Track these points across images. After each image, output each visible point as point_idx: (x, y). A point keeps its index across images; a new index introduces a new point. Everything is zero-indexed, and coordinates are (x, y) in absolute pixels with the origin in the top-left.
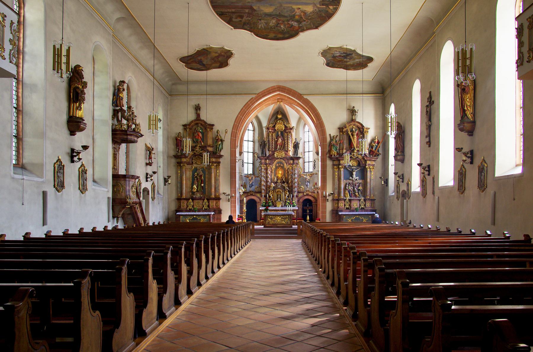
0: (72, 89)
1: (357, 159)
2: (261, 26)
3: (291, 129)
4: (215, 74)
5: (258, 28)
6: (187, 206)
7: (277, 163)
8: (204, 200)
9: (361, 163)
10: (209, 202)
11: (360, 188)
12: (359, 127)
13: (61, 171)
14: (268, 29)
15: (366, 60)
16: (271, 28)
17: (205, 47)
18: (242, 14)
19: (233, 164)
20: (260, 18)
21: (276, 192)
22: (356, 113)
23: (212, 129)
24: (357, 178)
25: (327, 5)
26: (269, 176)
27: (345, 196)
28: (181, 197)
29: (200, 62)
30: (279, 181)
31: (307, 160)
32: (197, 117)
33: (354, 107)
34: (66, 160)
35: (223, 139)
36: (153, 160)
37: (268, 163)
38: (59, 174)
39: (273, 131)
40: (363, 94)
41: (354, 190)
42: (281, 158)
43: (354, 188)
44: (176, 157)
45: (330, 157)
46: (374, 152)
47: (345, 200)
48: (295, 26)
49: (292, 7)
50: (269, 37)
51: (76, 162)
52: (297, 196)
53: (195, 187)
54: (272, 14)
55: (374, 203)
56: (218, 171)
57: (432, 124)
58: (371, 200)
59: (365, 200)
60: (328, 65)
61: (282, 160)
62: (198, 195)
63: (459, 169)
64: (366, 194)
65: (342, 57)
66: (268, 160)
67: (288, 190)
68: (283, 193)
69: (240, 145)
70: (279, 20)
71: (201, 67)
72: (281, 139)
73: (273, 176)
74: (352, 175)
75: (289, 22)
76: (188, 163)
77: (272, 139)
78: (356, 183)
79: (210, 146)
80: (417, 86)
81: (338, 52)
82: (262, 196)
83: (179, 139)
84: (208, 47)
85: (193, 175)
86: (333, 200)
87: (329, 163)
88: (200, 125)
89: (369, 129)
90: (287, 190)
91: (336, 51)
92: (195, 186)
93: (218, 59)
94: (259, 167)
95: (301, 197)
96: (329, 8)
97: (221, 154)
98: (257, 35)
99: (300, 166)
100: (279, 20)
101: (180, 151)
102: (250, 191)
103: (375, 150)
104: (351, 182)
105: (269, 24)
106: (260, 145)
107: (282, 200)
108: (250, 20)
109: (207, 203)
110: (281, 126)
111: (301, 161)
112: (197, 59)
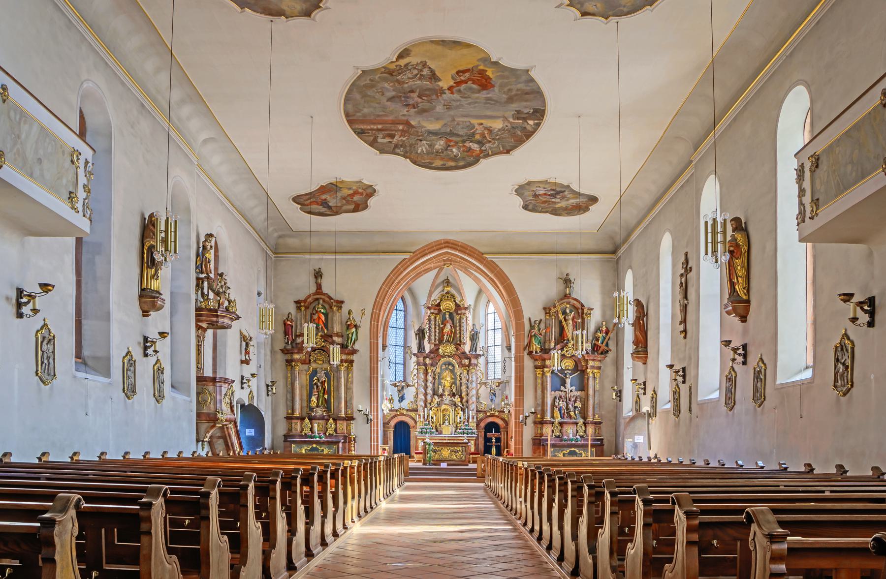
0: (146, 248)
1: (574, 358)
2: (422, 150)
3: (466, 308)
4: (346, 221)
5: (417, 153)
6: (302, 430)
8: (328, 420)
9: (579, 365)
10: (336, 424)
11: (578, 404)
12: (576, 306)
13: (132, 369)
14: (433, 153)
15: (586, 202)
16: (437, 152)
17: (333, 181)
18: (393, 132)
19: (374, 364)
20: (420, 138)
21: (442, 410)
22: (572, 285)
23: (341, 307)
24: (573, 388)
25: (525, 119)
27: (553, 416)
28: (293, 414)
29: (325, 203)
30: (446, 393)
31: (491, 360)
32: (317, 289)
33: (567, 275)
34: (137, 353)
35: (358, 325)
36: (251, 355)
38: (129, 372)
39: (436, 312)
40: (580, 254)
41: (567, 408)
43: (567, 405)
44: (284, 351)
45: (530, 353)
46: (600, 347)
47: (553, 423)
48: (475, 149)
49: (470, 121)
50: (433, 165)
51: (151, 355)
53: (315, 400)
54: (438, 131)
55: (600, 428)
56: (350, 375)
57: (688, 303)
58: (595, 424)
59: (585, 424)
60: (526, 207)
62: (319, 412)
63: (727, 373)
64: (587, 413)
65: (549, 195)
67: (461, 408)
69: (383, 334)
70: (451, 141)
71: (326, 211)
73: (436, 385)
74: (564, 383)
75: (465, 144)
76: (303, 362)
77: (435, 324)
78: (571, 396)
79: (337, 335)
80: (667, 242)
81: (542, 189)
83: (289, 323)
84: (338, 180)
85: (311, 380)
86: (535, 423)
87: (528, 363)
88: (321, 301)
89: (592, 309)
91: (540, 187)
92: (314, 399)
93: (352, 199)
94: (415, 370)
95: (482, 420)
96: (528, 124)
97: (355, 348)
98: (415, 163)
99: (482, 370)
100: (451, 141)
101: (290, 342)
103: (602, 343)
104: (563, 394)
105: (434, 147)
106: (416, 334)
107: (451, 423)
108: (404, 141)
109: (334, 426)
111: (482, 360)
112: (320, 199)
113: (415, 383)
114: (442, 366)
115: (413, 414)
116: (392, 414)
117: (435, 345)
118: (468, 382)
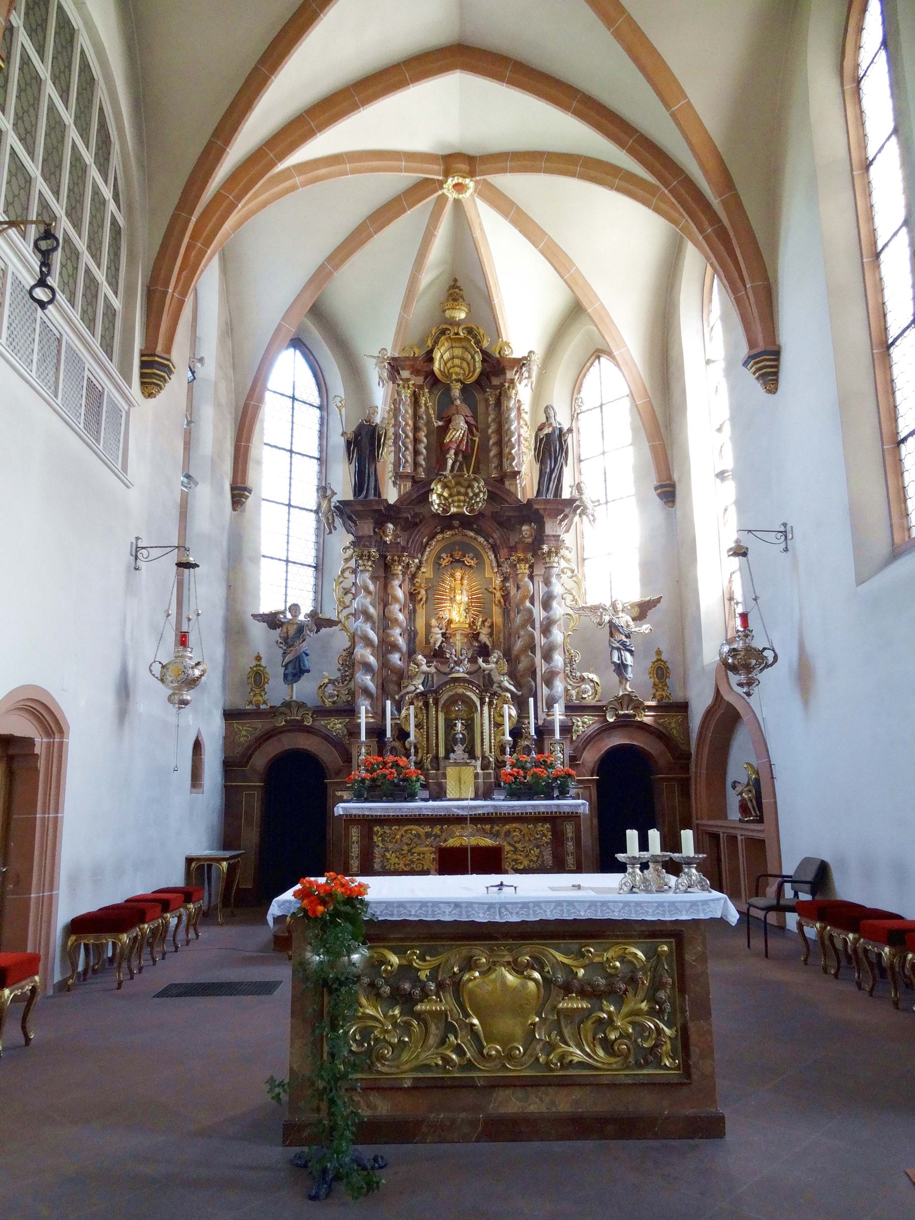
7: (442, 550)
21: (442, 702)
26: (401, 617)
37: (395, 544)
39: (420, 380)
42: (465, 522)
52: (566, 729)
61: (472, 534)
66: (391, 526)
68: (486, 708)
72: (467, 422)
73: (420, 623)
82: (353, 732)
90: (508, 690)
94: (347, 574)
95: (590, 740)
99: (574, 567)
102: (287, 705)
107: (478, 753)
110: (463, 359)
113: (347, 617)
114: (439, 557)
115: (336, 725)
116: (260, 726)
117: (415, 481)
118: (532, 603)
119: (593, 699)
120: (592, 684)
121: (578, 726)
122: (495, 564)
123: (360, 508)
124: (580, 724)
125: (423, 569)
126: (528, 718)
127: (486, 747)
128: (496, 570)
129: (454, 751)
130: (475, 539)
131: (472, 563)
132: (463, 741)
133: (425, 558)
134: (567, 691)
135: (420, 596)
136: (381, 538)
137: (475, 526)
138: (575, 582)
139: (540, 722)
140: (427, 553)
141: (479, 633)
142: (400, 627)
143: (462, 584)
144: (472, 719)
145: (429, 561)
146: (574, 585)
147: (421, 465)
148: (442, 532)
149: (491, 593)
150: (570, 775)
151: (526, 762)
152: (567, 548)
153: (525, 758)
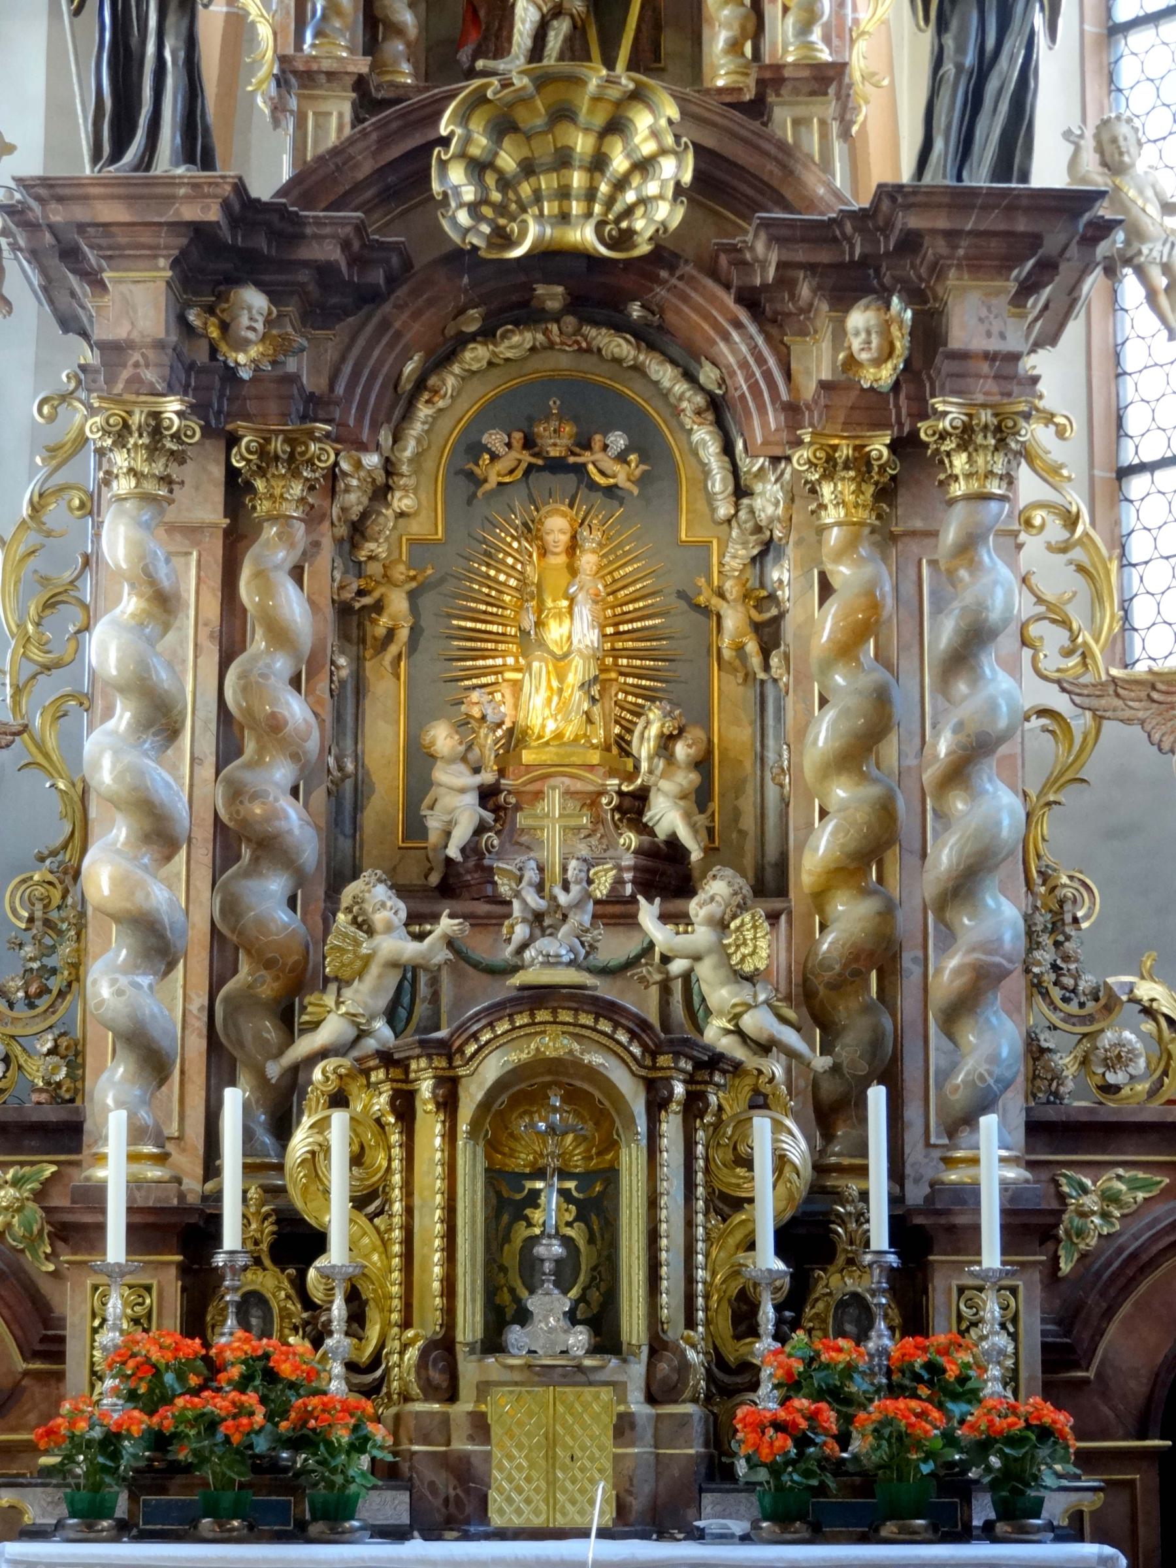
21: (472, 1096)
61: (621, 347)
90: (764, 1047)
99: (1077, 501)
119: (1153, 1093)
120: (1148, 1026)
121: (1084, 1214)
122: (719, 482)
123: (113, 212)
124: (1091, 1202)
125: (401, 501)
126: (862, 1171)
127: (670, 1301)
128: (724, 510)
129: (523, 1317)
130: (638, 369)
131: (621, 475)
132: (564, 1276)
133: (410, 448)
134: (1035, 1052)
135: (384, 621)
136: (213, 351)
137: (636, 311)
138: (1081, 569)
139: (915, 1194)
140: (416, 429)
141: (641, 797)
142: (295, 757)
143: (573, 571)
144: (611, 1175)
145: (429, 464)
146: (1080, 581)
147: (397, 30)
148: (487, 334)
149: (705, 611)
150: (1045, 1433)
151: (849, 1370)
152: (1049, 418)
153: (843, 1351)
